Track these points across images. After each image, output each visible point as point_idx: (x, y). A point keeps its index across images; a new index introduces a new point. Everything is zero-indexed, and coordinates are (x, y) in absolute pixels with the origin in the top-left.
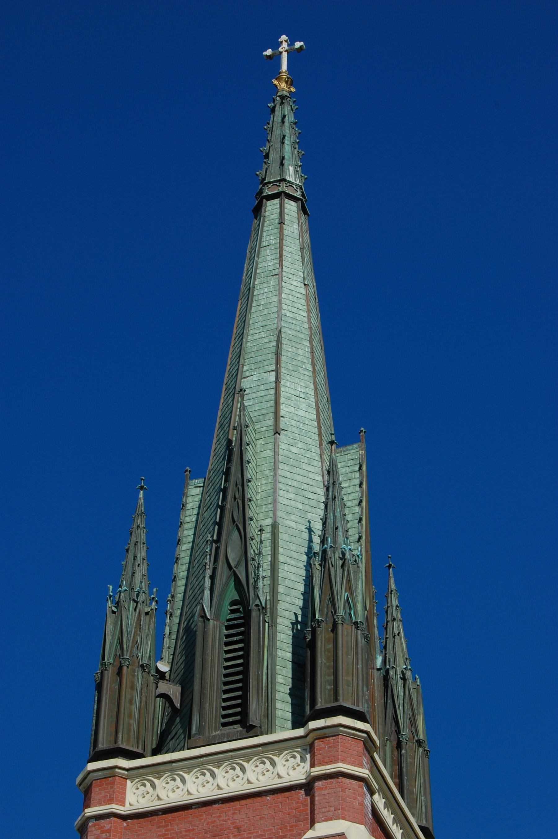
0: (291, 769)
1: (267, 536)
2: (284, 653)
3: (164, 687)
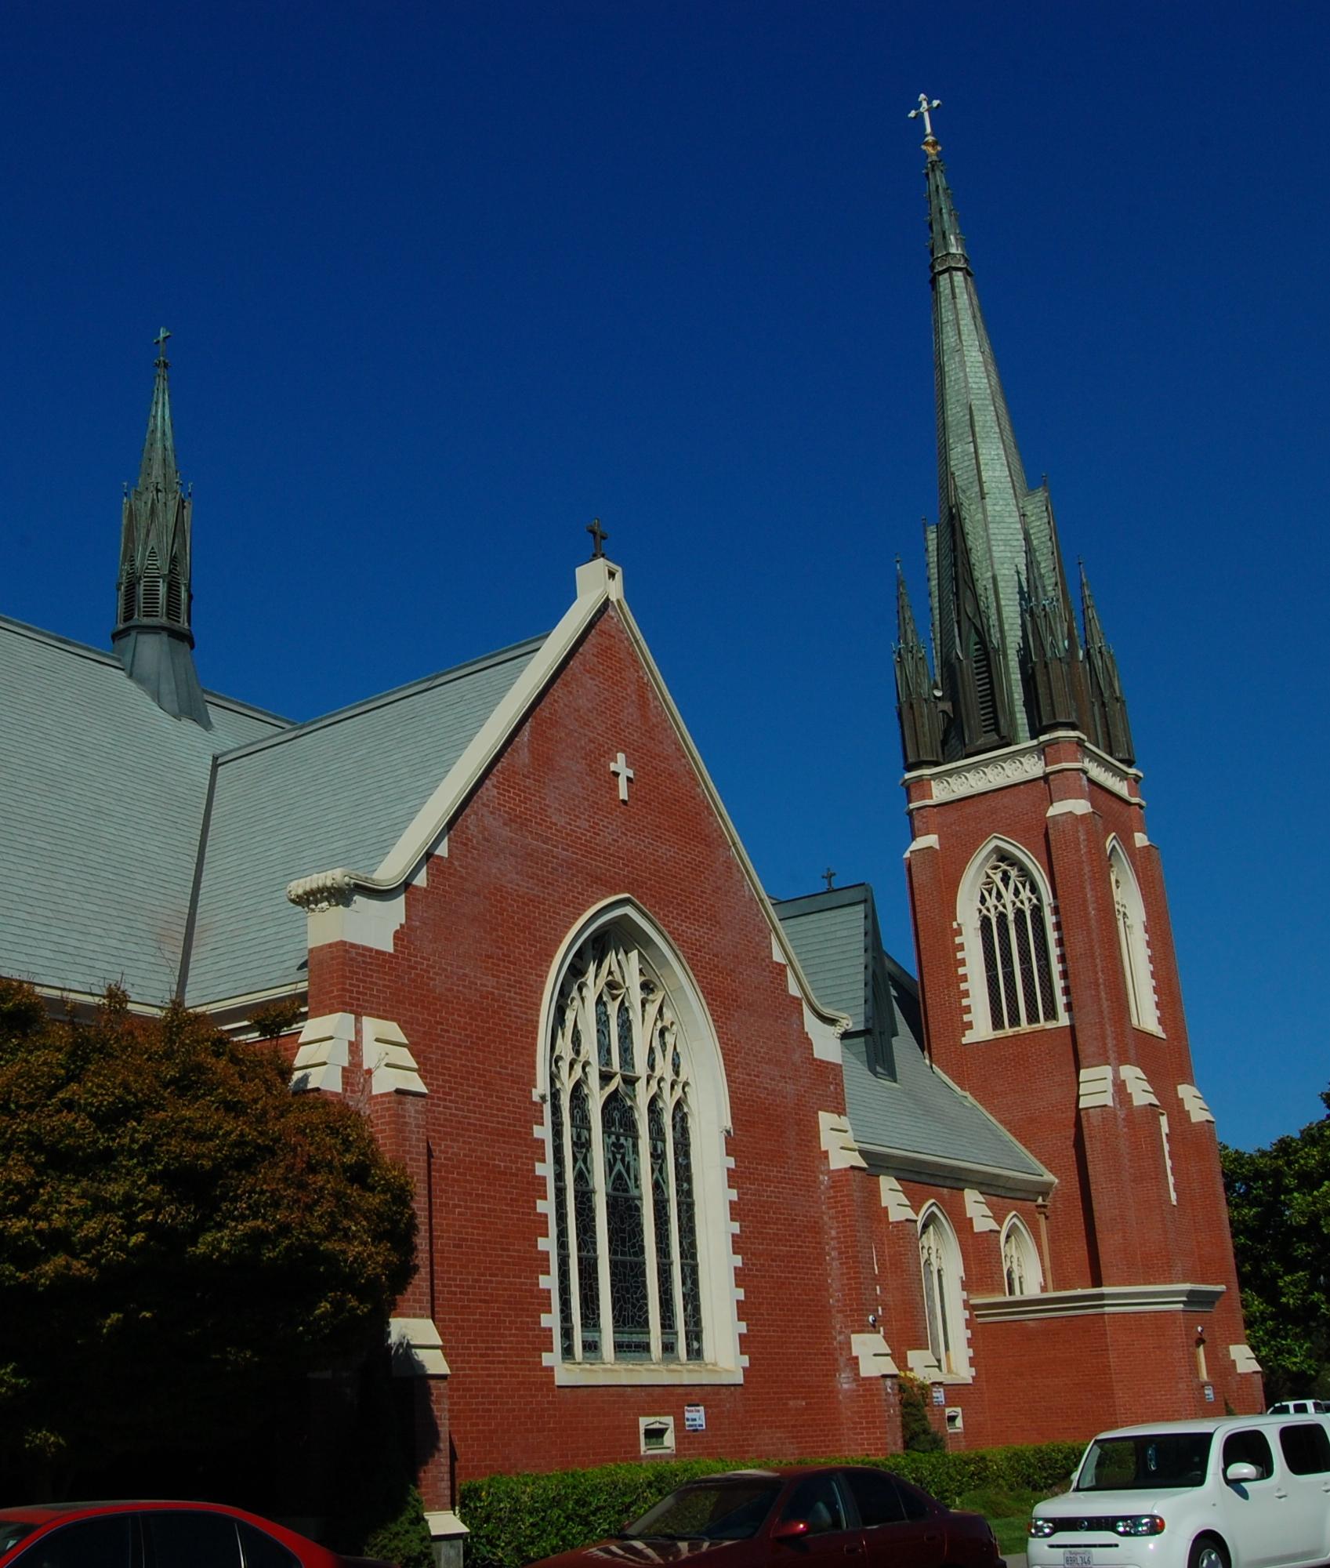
0: (1033, 767)
1: (990, 586)
2: (1016, 676)
3: (942, 706)
